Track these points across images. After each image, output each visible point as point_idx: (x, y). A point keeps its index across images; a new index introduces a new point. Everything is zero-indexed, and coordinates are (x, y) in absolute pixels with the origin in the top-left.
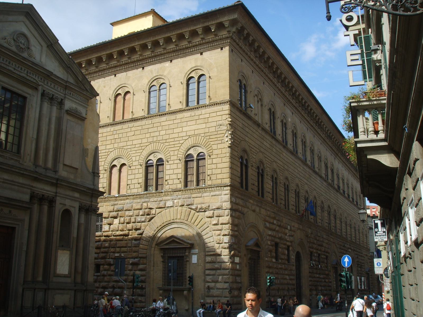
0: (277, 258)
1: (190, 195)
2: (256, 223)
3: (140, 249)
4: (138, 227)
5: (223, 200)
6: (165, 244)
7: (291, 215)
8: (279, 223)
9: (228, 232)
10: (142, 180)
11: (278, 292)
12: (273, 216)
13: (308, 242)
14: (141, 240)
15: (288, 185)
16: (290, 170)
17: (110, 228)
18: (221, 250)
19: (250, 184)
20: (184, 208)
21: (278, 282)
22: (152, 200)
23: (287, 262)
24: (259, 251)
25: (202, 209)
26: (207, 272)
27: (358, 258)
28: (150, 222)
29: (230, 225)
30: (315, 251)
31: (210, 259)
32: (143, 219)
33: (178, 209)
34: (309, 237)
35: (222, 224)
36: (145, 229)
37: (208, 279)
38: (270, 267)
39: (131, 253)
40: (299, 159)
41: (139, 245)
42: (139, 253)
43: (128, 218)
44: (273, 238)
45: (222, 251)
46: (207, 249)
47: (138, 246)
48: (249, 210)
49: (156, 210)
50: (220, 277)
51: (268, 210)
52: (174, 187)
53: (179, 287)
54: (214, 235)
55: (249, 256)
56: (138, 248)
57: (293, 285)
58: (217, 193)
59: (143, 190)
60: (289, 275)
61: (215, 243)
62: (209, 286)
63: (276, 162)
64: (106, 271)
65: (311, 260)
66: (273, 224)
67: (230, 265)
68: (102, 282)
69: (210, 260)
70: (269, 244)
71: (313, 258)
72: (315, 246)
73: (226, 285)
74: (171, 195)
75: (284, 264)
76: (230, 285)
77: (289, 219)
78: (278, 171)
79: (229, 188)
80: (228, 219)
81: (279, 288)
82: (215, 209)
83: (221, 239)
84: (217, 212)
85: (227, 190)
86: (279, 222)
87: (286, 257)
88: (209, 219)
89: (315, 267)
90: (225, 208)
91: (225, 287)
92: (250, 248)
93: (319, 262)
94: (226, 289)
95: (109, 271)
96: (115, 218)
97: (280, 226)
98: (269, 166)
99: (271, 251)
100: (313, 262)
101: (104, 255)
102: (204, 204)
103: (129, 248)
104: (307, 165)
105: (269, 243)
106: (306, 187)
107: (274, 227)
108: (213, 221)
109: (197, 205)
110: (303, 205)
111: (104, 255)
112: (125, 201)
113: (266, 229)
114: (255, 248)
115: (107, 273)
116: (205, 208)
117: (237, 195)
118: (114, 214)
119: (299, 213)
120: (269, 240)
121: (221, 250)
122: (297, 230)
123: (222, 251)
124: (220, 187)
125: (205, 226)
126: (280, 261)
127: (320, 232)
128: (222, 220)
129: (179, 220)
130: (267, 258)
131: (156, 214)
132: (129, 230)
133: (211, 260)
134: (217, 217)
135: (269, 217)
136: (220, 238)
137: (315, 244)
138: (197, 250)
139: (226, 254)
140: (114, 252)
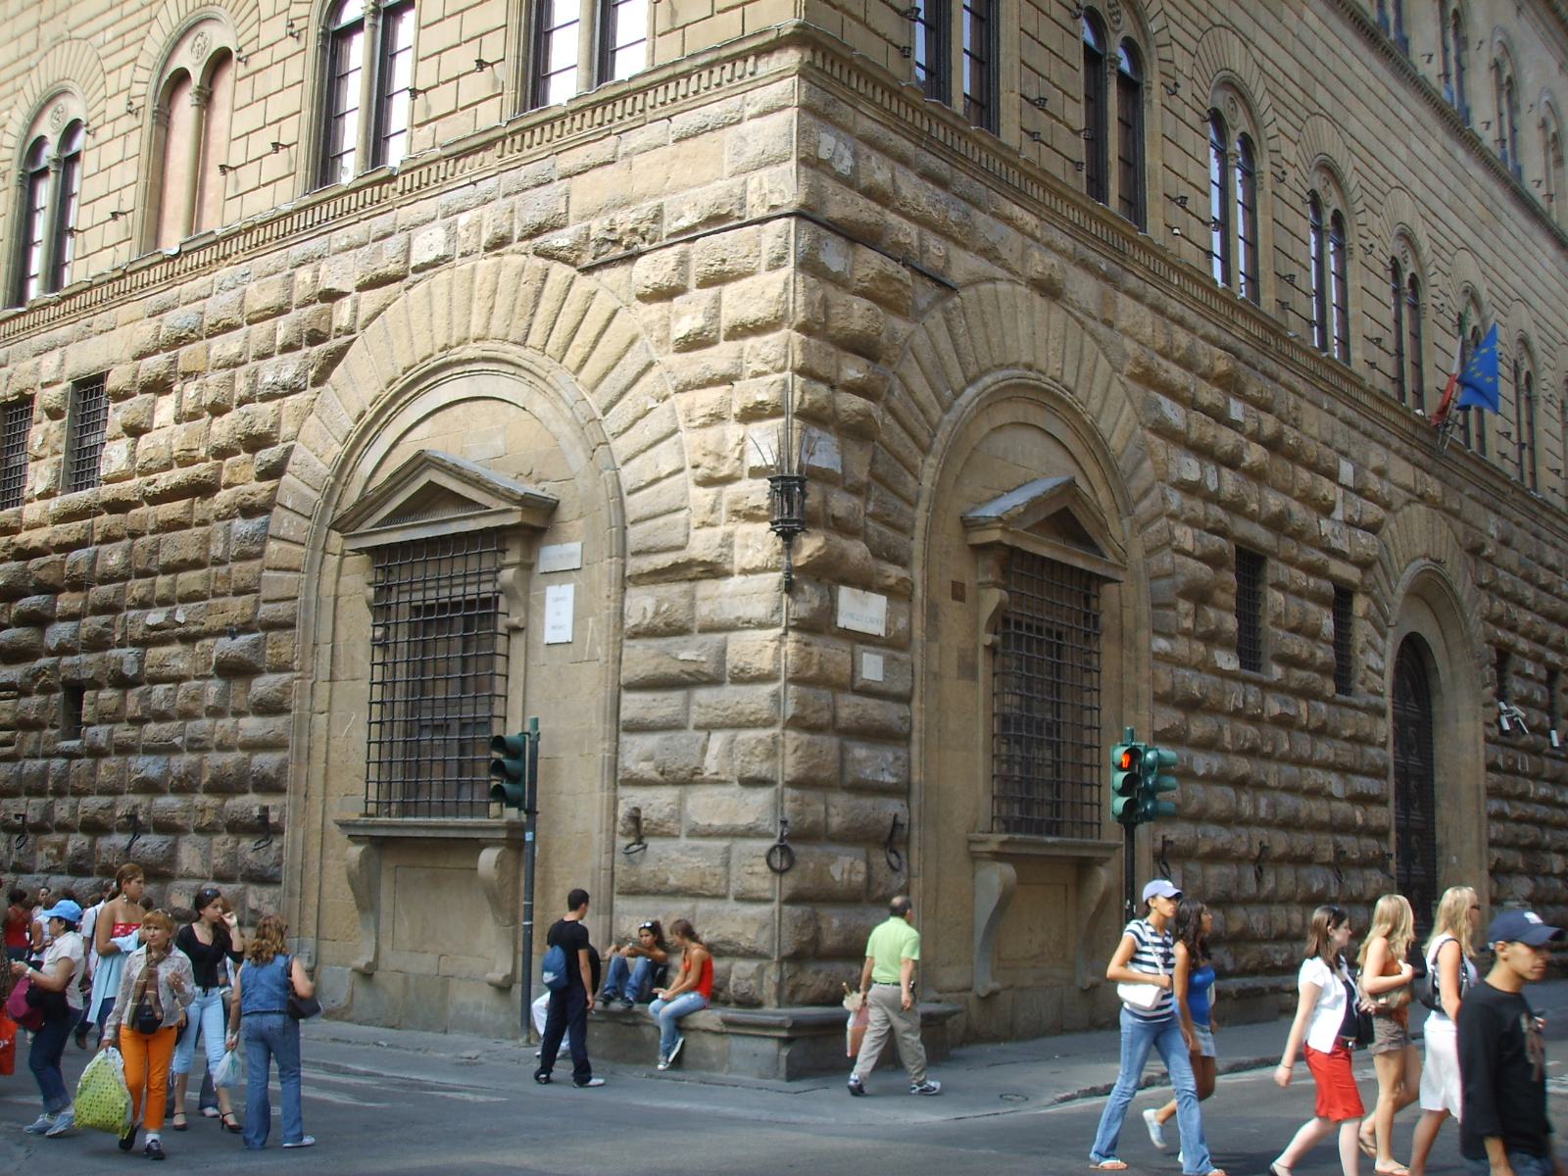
0: (1249, 648)
1: (546, 164)
2: (1069, 379)
3: (268, 569)
4: (260, 427)
5: (751, 152)
6: (378, 525)
7: (1364, 398)
8: (1269, 425)
9: (777, 387)
10: (297, 131)
11: (1259, 878)
12: (1222, 366)
13: (1482, 586)
14: (277, 509)
15: (1337, 217)
16: (1354, 126)
17: (132, 457)
18: (729, 528)
19: (1015, 97)
20: (512, 259)
21: (1256, 808)
22: (340, 239)
23: (1330, 687)
24: (1090, 575)
25: (615, 242)
26: (634, 705)
28: (327, 386)
29: (797, 337)
30: (1523, 645)
31: (649, 603)
32: (285, 368)
33: (474, 268)
34: (1489, 559)
35: (742, 331)
36: (295, 438)
37: (638, 752)
38: (1192, 705)
39: (221, 600)
40: (1419, 85)
41: (263, 543)
42: (265, 594)
43: (215, 378)
44: (1216, 512)
45: (737, 541)
46: (636, 536)
47: (257, 549)
48: (1000, 273)
49: (356, 301)
50: (717, 741)
51: (1181, 322)
52: (458, 128)
53: (450, 820)
54: (681, 419)
55: (994, 598)
56: (255, 564)
57: (1380, 834)
58: (715, 111)
59: (300, 189)
60: (1344, 770)
61: (690, 481)
62: (635, 817)
63: (1247, 42)
64: (110, 722)
65: (1501, 694)
66: (1220, 416)
67: (790, 646)
68: (87, 793)
69: (650, 615)
70: (1188, 545)
71: (1517, 686)
72: (1525, 618)
73: (755, 806)
74: (443, 184)
75: (1308, 694)
76: (778, 803)
77: (1351, 424)
78: (1262, 100)
79: (790, 59)
80: (775, 290)
81: (1263, 849)
82: (692, 228)
83: (732, 442)
84: (706, 252)
85: (781, 76)
86: (1263, 415)
87: (1320, 654)
88: (656, 306)
89: (1529, 738)
90: (761, 212)
91: (744, 820)
92: (995, 535)
93: (1550, 709)
94: (750, 833)
95: (119, 721)
96: (159, 386)
97: (1274, 445)
98: (1192, 45)
99: (1200, 595)
100: (1515, 708)
101: (93, 623)
102: (628, 204)
103: (214, 569)
104: (1471, 142)
105: (1185, 536)
106: (1468, 269)
107: (1227, 439)
108: (678, 315)
109: (586, 224)
110: (1443, 359)
111: (93, 623)
112: (211, 277)
113: (1157, 441)
114: (1047, 549)
115: (111, 732)
116: (634, 231)
117: (867, 126)
118: (156, 364)
119: (1420, 405)
120: (1191, 522)
121: (729, 528)
122: (1409, 502)
123: (730, 535)
124: (733, 59)
125: (632, 364)
126: (1277, 672)
127: (1555, 546)
128: (743, 301)
129: (480, 344)
130: (1169, 636)
131: (358, 329)
132: (221, 453)
133: (656, 613)
134: (706, 283)
135: (1187, 364)
136: (723, 439)
137: (1528, 608)
138: (575, 547)
139: (758, 562)
140: (144, 604)
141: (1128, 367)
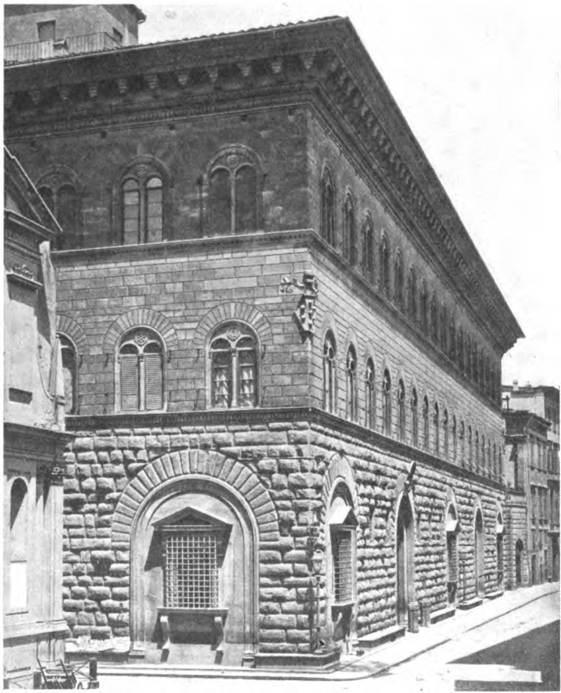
27: (485, 508)
51: (360, 445)
57: (393, 585)
97: (378, 472)
141: (352, 465)
